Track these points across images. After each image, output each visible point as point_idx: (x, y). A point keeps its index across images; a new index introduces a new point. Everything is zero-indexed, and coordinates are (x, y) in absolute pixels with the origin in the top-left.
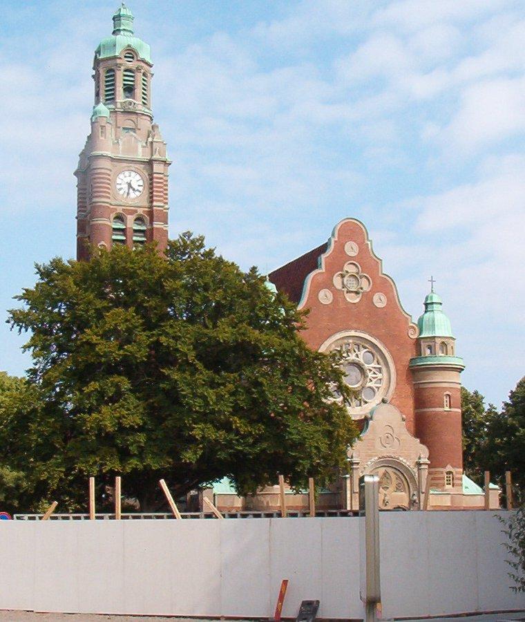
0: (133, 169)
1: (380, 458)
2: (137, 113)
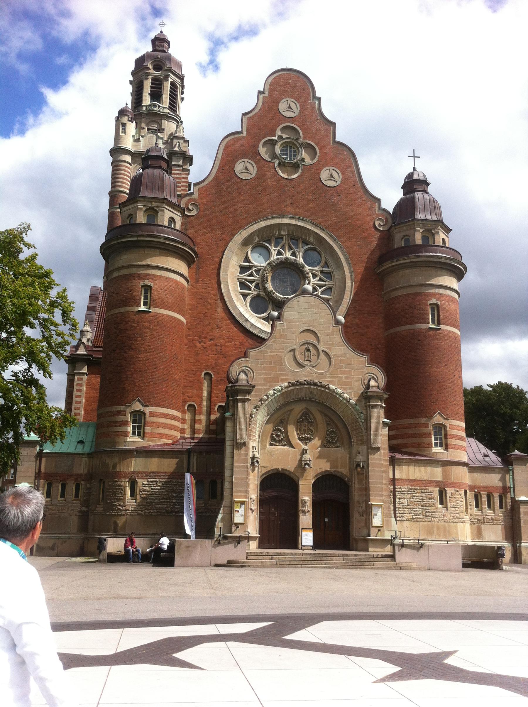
1: (293, 385)
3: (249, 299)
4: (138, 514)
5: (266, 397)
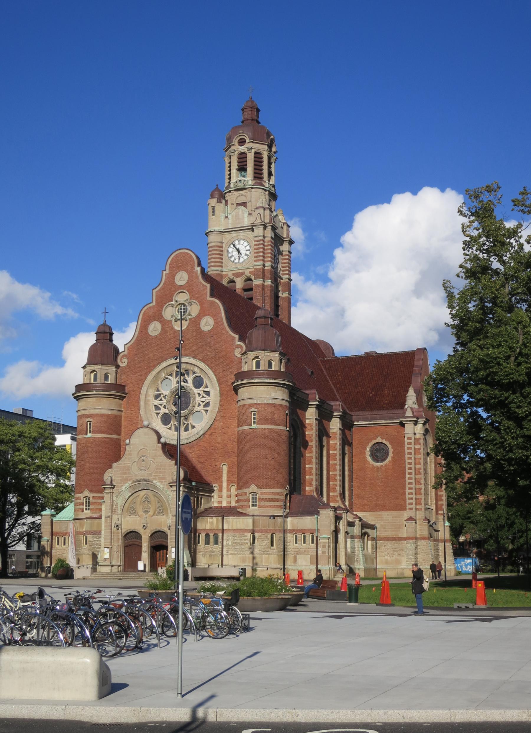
0: (242, 237)
1: (134, 482)
2: (246, 189)
3: (160, 416)
4: (88, 554)
5: (121, 490)
